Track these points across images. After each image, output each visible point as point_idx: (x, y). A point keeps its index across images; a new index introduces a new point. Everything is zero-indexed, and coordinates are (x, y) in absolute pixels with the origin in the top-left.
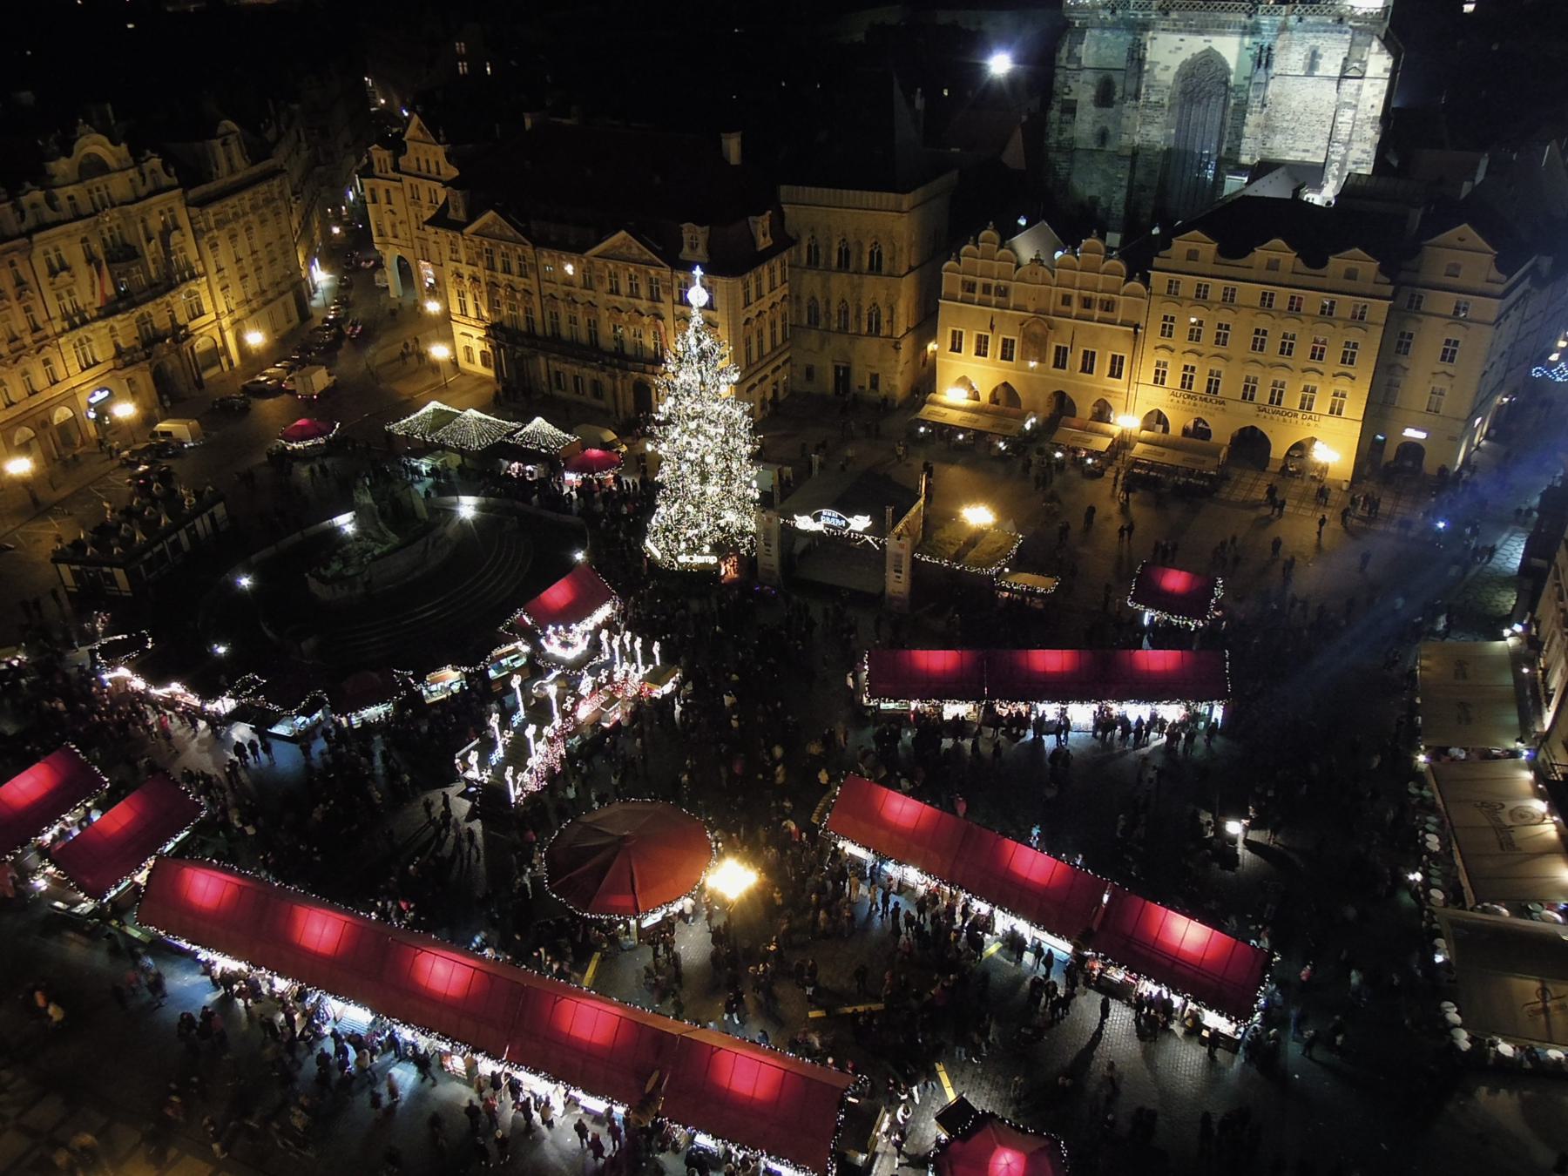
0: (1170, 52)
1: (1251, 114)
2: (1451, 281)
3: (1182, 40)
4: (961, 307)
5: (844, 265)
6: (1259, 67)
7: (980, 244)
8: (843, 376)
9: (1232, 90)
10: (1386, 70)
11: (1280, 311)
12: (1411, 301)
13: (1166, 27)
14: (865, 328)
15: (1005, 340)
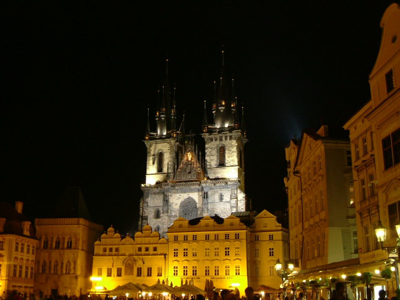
0: (177, 199)
1: (204, 213)
2: (266, 229)
3: (180, 195)
4: (102, 258)
5: (57, 247)
6: (204, 198)
7: (108, 233)
8: (55, 292)
9: (198, 209)
10: (243, 198)
11: (212, 241)
12: (256, 238)
13: (175, 192)
14: (64, 272)
15: (118, 269)
